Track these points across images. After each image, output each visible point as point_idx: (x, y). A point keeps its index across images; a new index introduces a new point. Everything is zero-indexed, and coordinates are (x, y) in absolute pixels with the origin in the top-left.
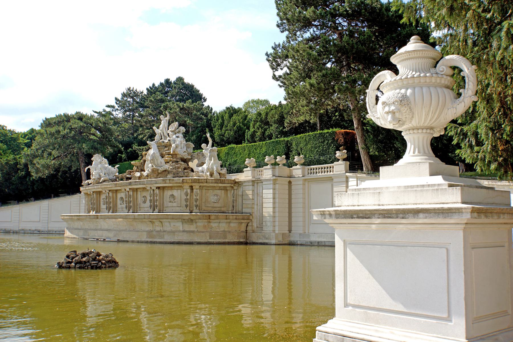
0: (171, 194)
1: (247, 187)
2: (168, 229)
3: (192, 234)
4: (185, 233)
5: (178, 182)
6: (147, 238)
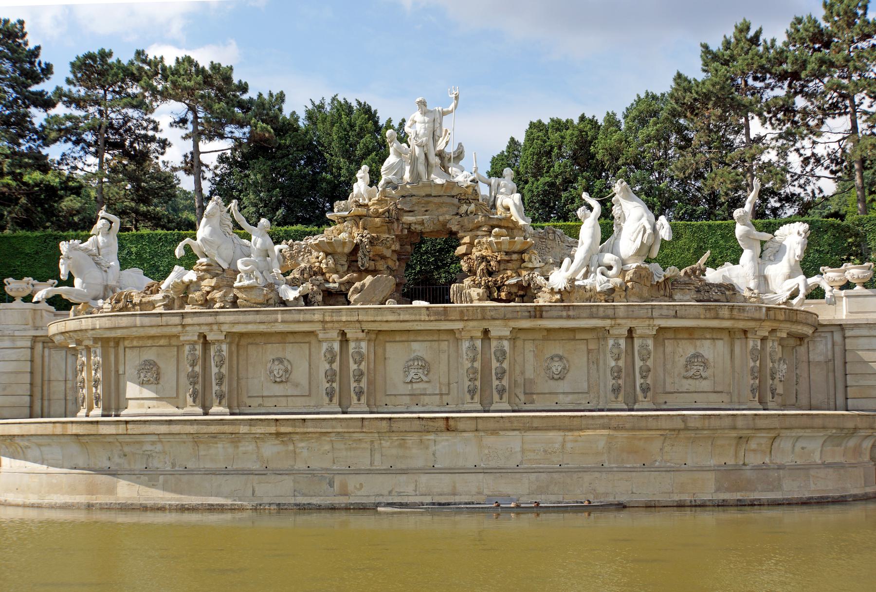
0: (691, 351)
1: (862, 341)
2: (787, 460)
3: (842, 472)
4: (831, 470)
5: (757, 315)
6: (718, 490)
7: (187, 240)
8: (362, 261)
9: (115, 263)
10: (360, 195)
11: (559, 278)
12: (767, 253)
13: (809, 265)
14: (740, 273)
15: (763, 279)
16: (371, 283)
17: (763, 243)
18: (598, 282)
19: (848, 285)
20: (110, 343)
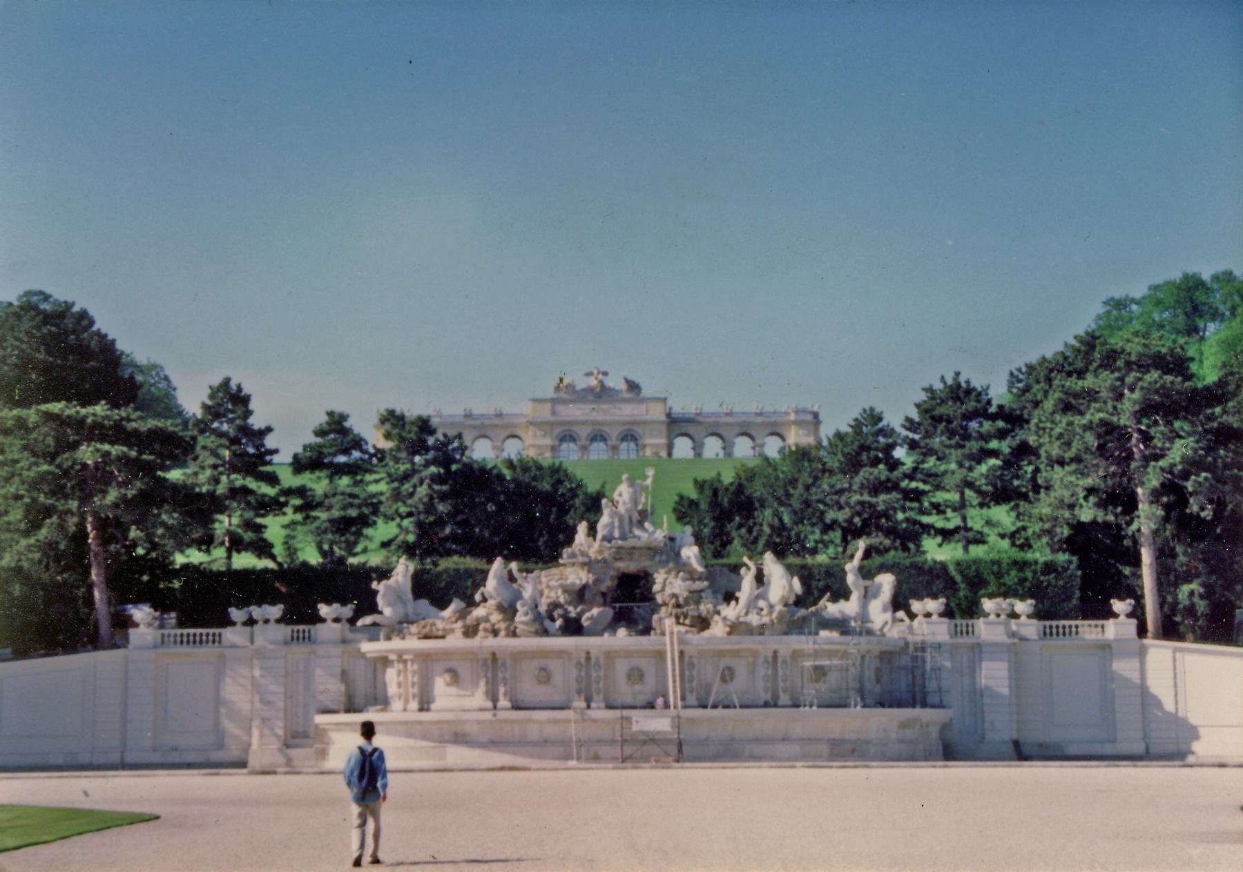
7: (482, 589)
8: (588, 595)
9: (410, 596)
10: (581, 544)
12: (867, 595)
13: (899, 603)
14: (849, 608)
16: (599, 613)
17: (866, 588)
19: (928, 615)
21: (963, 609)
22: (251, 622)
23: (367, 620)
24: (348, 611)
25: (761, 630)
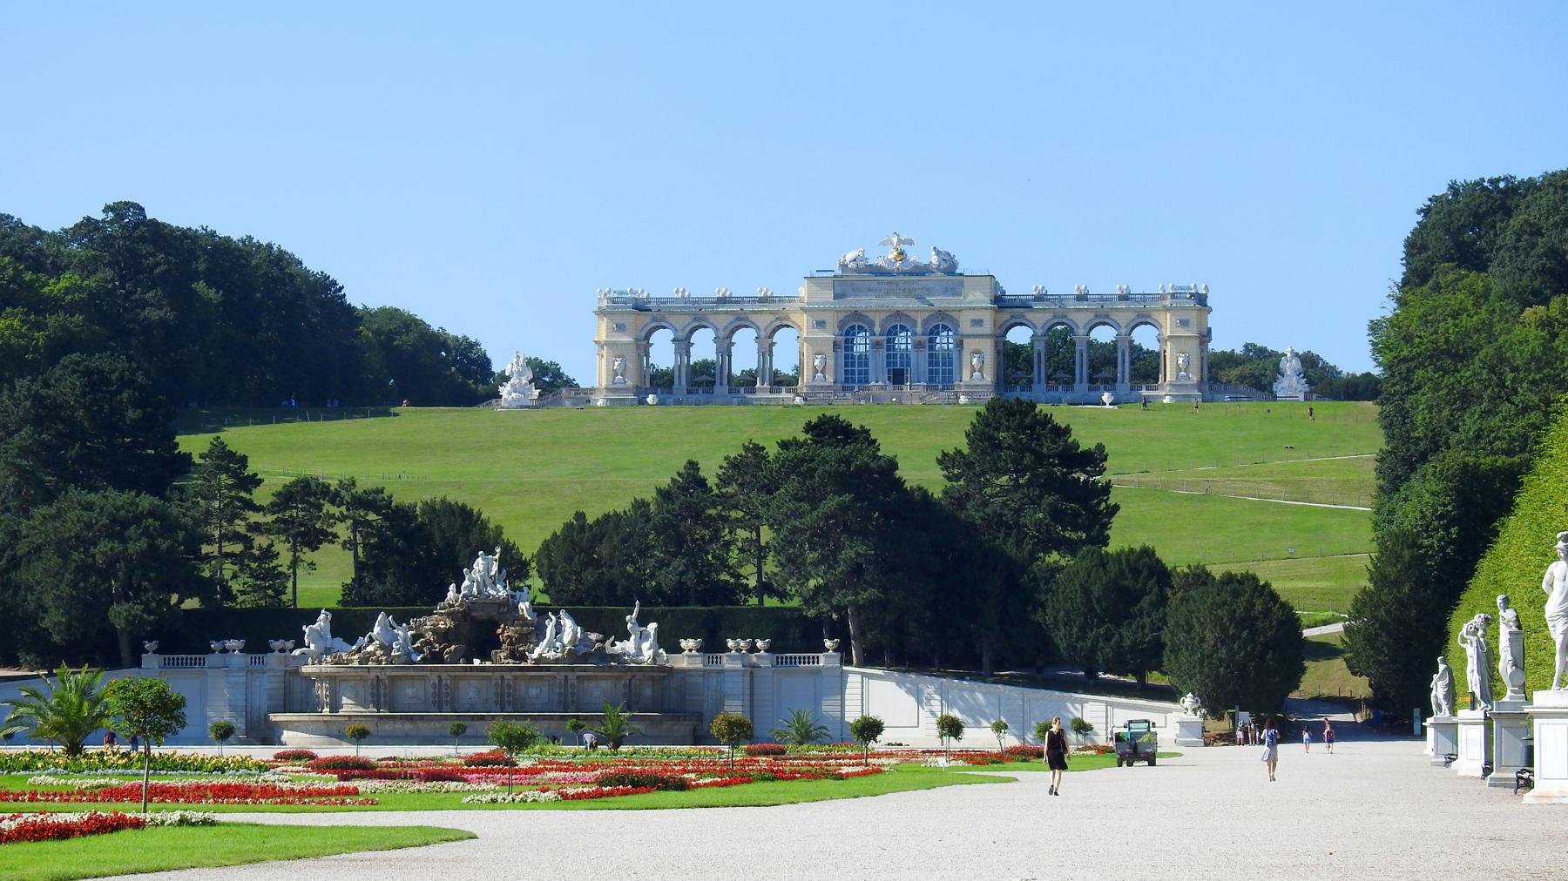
11: (538, 651)
14: (629, 646)
15: (639, 651)
18: (551, 655)
20: (331, 678)
21: (713, 646)
22: (224, 651)
23: (297, 652)
24: (290, 644)
25: (557, 661)
